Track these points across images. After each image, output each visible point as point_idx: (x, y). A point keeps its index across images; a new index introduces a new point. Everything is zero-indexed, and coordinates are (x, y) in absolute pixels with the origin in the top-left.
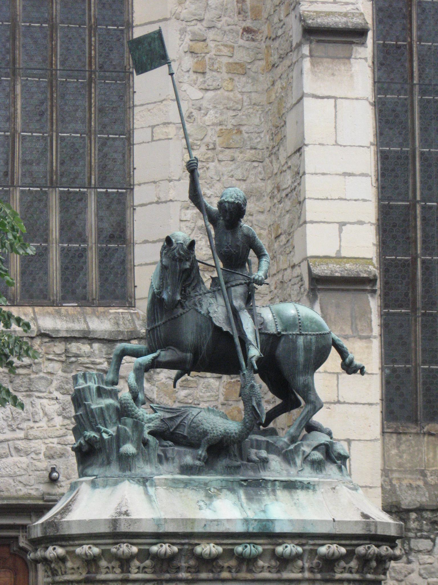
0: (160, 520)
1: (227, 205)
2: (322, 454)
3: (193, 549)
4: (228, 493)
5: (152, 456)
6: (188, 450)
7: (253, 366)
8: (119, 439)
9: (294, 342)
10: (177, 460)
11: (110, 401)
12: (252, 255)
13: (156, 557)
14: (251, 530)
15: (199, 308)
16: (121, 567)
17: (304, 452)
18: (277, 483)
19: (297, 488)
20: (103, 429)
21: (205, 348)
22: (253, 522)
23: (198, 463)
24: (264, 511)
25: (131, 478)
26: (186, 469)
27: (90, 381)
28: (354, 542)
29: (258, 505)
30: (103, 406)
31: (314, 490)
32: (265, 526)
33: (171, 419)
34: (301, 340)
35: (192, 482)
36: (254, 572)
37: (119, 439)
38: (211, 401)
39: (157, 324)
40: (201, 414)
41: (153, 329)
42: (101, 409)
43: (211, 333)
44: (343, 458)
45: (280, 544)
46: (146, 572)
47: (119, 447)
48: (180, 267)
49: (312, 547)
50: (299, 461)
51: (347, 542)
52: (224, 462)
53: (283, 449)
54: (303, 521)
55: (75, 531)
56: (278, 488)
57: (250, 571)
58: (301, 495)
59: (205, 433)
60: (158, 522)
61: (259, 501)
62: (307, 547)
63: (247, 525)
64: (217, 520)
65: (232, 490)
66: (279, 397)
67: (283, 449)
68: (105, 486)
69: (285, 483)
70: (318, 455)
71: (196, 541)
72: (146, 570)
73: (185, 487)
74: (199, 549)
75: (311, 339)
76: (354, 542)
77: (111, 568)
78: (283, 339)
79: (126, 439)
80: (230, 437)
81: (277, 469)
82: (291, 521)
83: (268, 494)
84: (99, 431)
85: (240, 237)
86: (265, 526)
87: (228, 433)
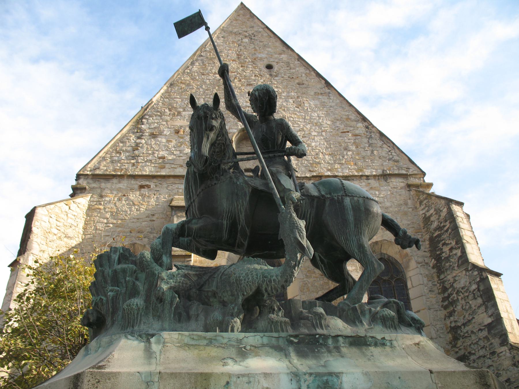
0: (151, 374)
5: (166, 311)
9: (341, 202)
10: (202, 317)
15: (235, 180)
18: (340, 339)
19: (370, 345)
21: (242, 217)
22: (307, 377)
24: (324, 366)
29: (314, 362)
32: (327, 382)
34: (347, 201)
35: (218, 338)
48: (206, 124)
54: (384, 373)
56: (343, 345)
63: (299, 381)
64: (248, 375)
69: (351, 339)
73: (207, 345)
75: (358, 201)
78: (327, 203)
79: (134, 293)
83: (329, 351)
86: (327, 382)
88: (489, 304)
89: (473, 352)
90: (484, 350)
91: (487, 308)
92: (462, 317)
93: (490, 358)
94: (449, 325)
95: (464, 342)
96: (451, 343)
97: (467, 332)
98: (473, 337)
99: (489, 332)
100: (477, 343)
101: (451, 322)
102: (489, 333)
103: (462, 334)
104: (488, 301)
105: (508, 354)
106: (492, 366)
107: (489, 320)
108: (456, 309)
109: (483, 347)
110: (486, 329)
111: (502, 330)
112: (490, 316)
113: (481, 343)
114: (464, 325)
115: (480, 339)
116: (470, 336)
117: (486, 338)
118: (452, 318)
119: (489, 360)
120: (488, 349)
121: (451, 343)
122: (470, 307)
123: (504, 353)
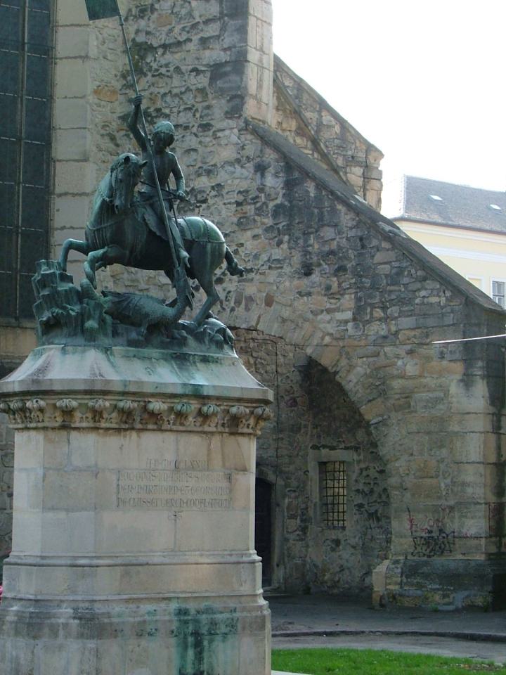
0: (126, 381)
1: (163, 135)
3: (145, 406)
4: (164, 362)
6: (133, 328)
7: (186, 265)
8: (82, 317)
9: (204, 247)
13: (122, 411)
14: (187, 393)
16: (94, 418)
18: (196, 357)
19: (209, 362)
23: (140, 338)
25: (97, 347)
26: (131, 343)
27: (53, 267)
28: (254, 405)
30: (67, 288)
31: (221, 364)
33: (119, 302)
34: (209, 246)
36: (184, 425)
37: (82, 317)
38: (152, 288)
39: (103, 226)
40: (142, 300)
41: (98, 230)
42: (66, 290)
43: (145, 236)
45: (204, 405)
46: (111, 423)
49: (225, 407)
50: (207, 340)
51: (249, 405)
52: (156, 339)
53: (194, 331)
55: (57, 387)
57: (182, 424)
58: (212, 366)
59: (147, 315)
60: (125, 383)
61: (187, 370)
62: (222, 407)
65: (166, 360)
67: (194, 331)
68: (74, 353)
69: (201, 358)
71: (150, 400)
72: (112, 420)
74: (151, 406)
76: (254, 405)
78: (195, 245)
81: (193, 347)
82: (214, 386)
84: (64, 308)
85: (167, 162)
87: (165, 314)
88: (232, 23)
89: (167, 111)
90: (190, 114)
91: (223, 29)
92: (166, 29)
93: (196, 135)
94: (132, 36)
95: (153, 84)
96: (124, 76)
97: (167, 65)
98: (176, 81)
99: (213, 80)
100: (179, 96)
101: (137, 32)
102: (210, 84)
103: (154, 66)
104: (232, 16)
105: (234, 139)
106: (195, 150)
107: (224, 57)
108: (157, 6)
109: (190, 109)
110: (208, 74)
111: (239, 88)
112: (225, 50)
113: (189, 99)
114: (165, 47)
115: (188, 89)
116: (171, 77)
117: (202, 91)
118: (142, 23)
119: (194, 138)
120: (198, 115)
121: (124, 76)
122: (190, 14)
123: (227, 132)
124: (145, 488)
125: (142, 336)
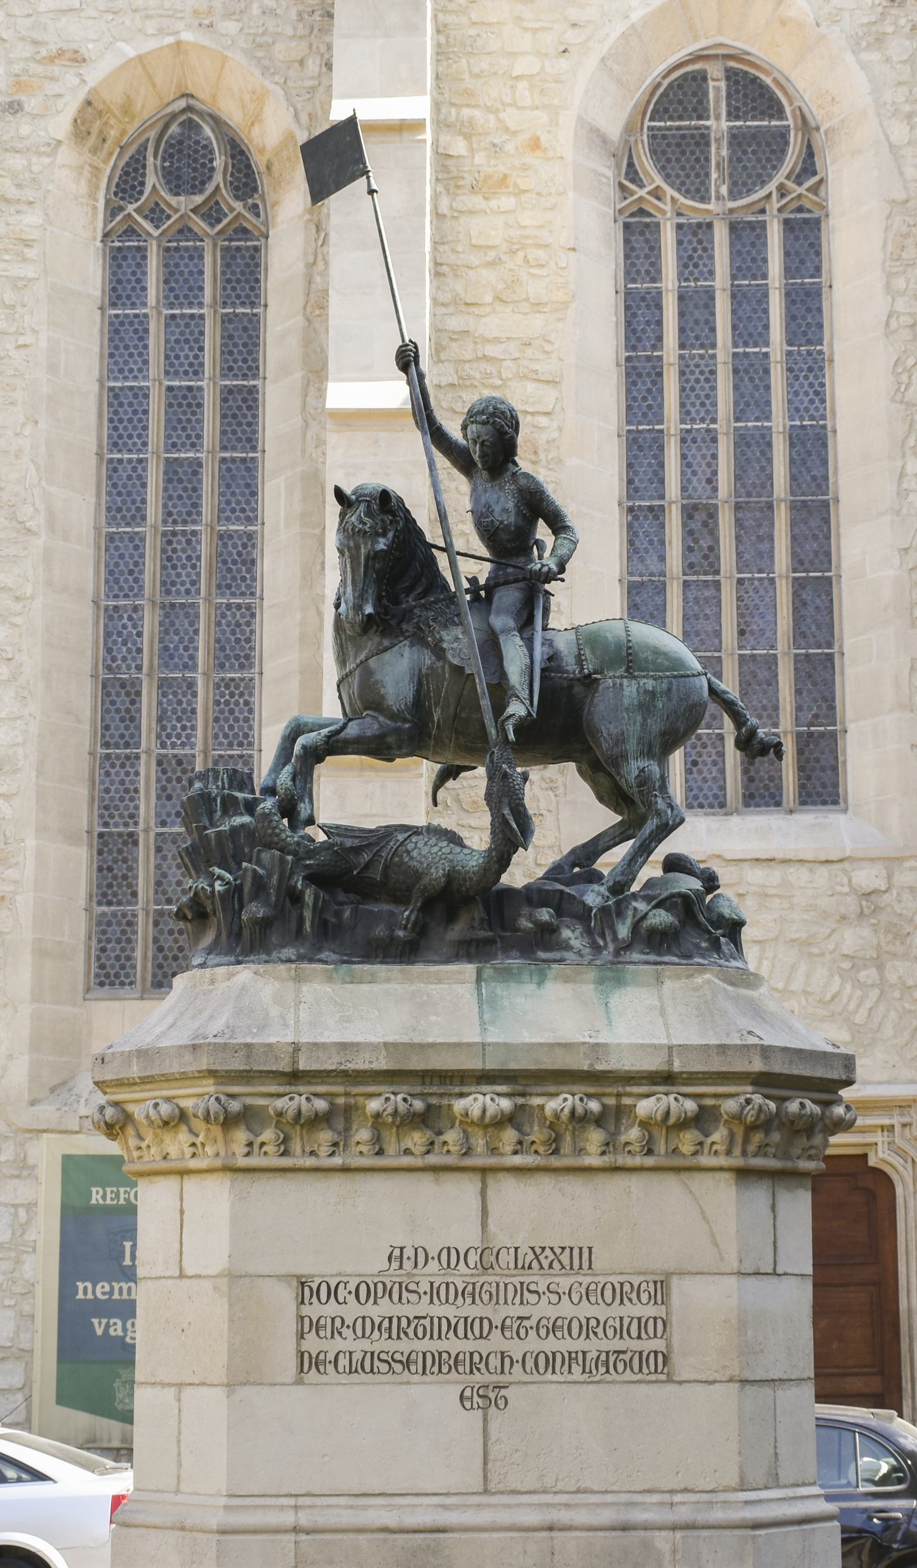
2: (677, 916)
11: (246, 819)
12: (543, 531)
17: (635, 909)
20: (217, 871)
33: (357, 850)
44: (734, 928)
47: (241, 907)
59: (418, 875)
66: (616, 811)
70: (661, 918)
72: (264, 1149)
77: (199, 1145)
80: (465, 879)
124: (386, 1324)
125: (405, 928)
